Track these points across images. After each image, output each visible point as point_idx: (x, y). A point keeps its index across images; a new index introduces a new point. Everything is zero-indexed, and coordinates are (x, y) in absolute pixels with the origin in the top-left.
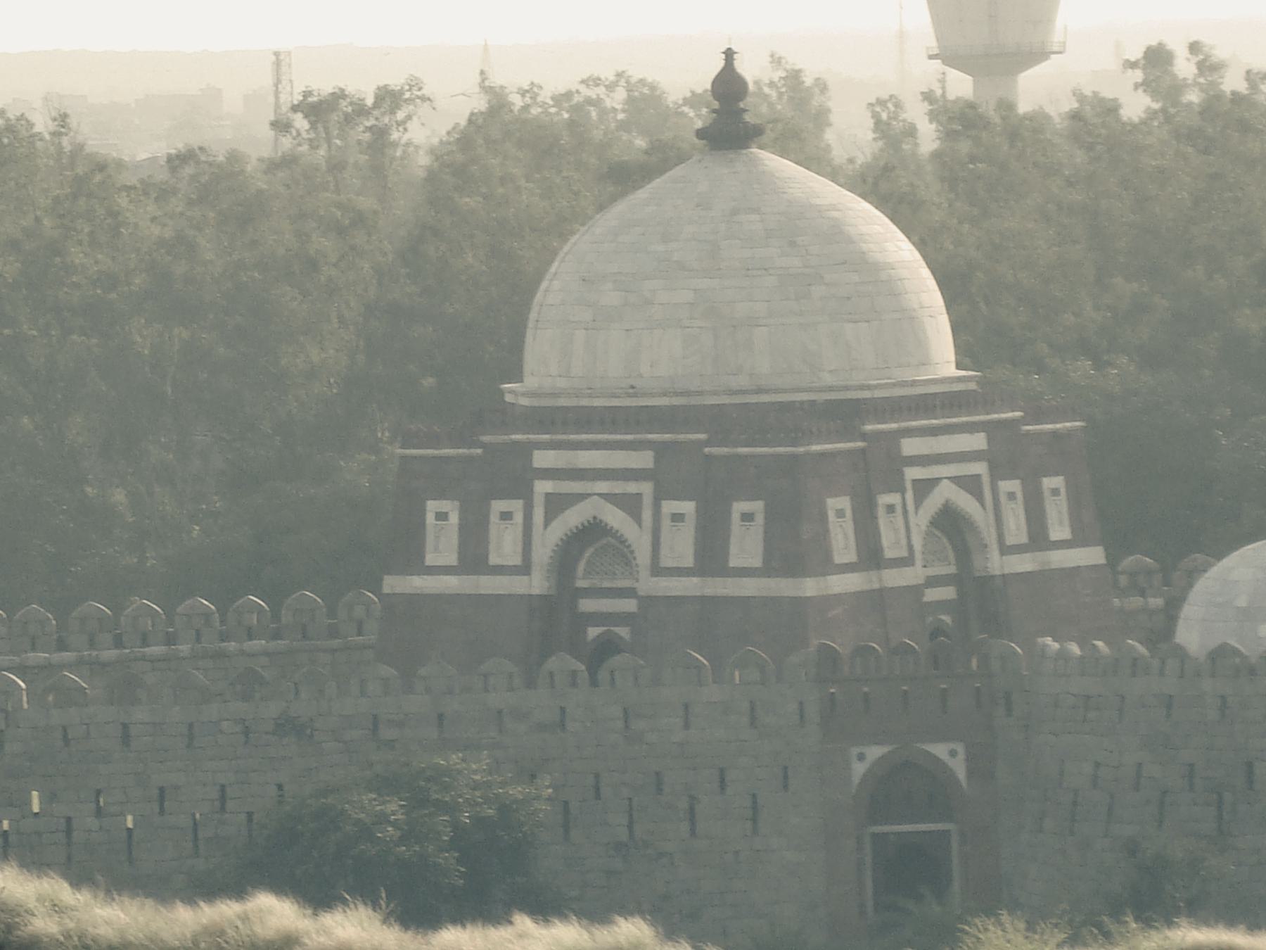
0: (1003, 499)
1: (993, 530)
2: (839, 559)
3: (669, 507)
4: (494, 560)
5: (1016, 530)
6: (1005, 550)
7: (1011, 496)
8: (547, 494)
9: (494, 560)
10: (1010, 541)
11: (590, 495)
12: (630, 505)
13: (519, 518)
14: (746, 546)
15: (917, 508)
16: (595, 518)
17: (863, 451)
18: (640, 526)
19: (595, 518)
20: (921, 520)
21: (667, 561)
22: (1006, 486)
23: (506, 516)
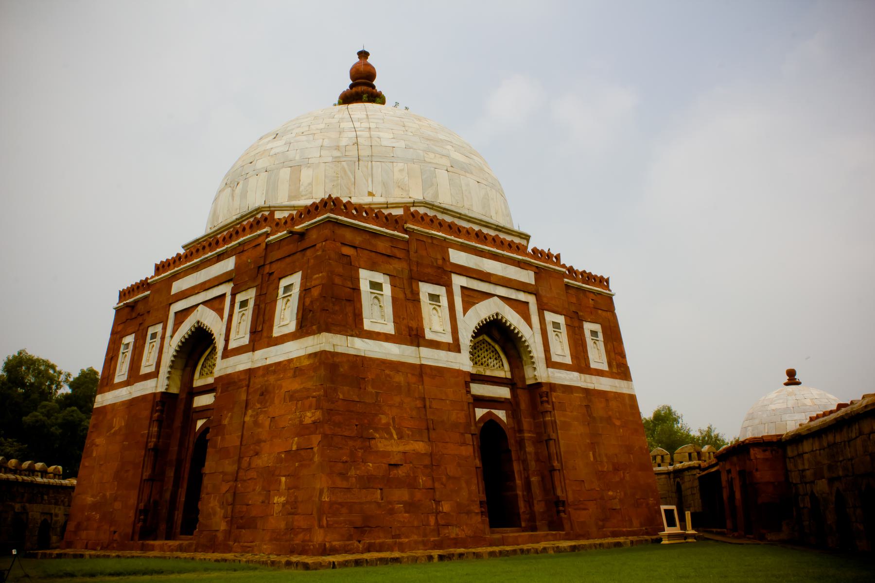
0: (550, 328)
1: (541, 348)
2: (367, 325)
3: (240, 298)
4: (144, 370)
5: (561, 350)
6: (550, 363)
7: (556, 325)
8: (176, 313)
9: (144, 370)
10: (555, 358)
11: (198, 305)
12: (215, 304)
13: (159, 336)
14: (286, 317)
15: (465, 311)
16: (198, 322)
17: (407, 242)
18: (222, 318)
19: (198, 322)
20: (470, 321)
21: (232, 345)
22: (550, 317)
23: (154, 336)
